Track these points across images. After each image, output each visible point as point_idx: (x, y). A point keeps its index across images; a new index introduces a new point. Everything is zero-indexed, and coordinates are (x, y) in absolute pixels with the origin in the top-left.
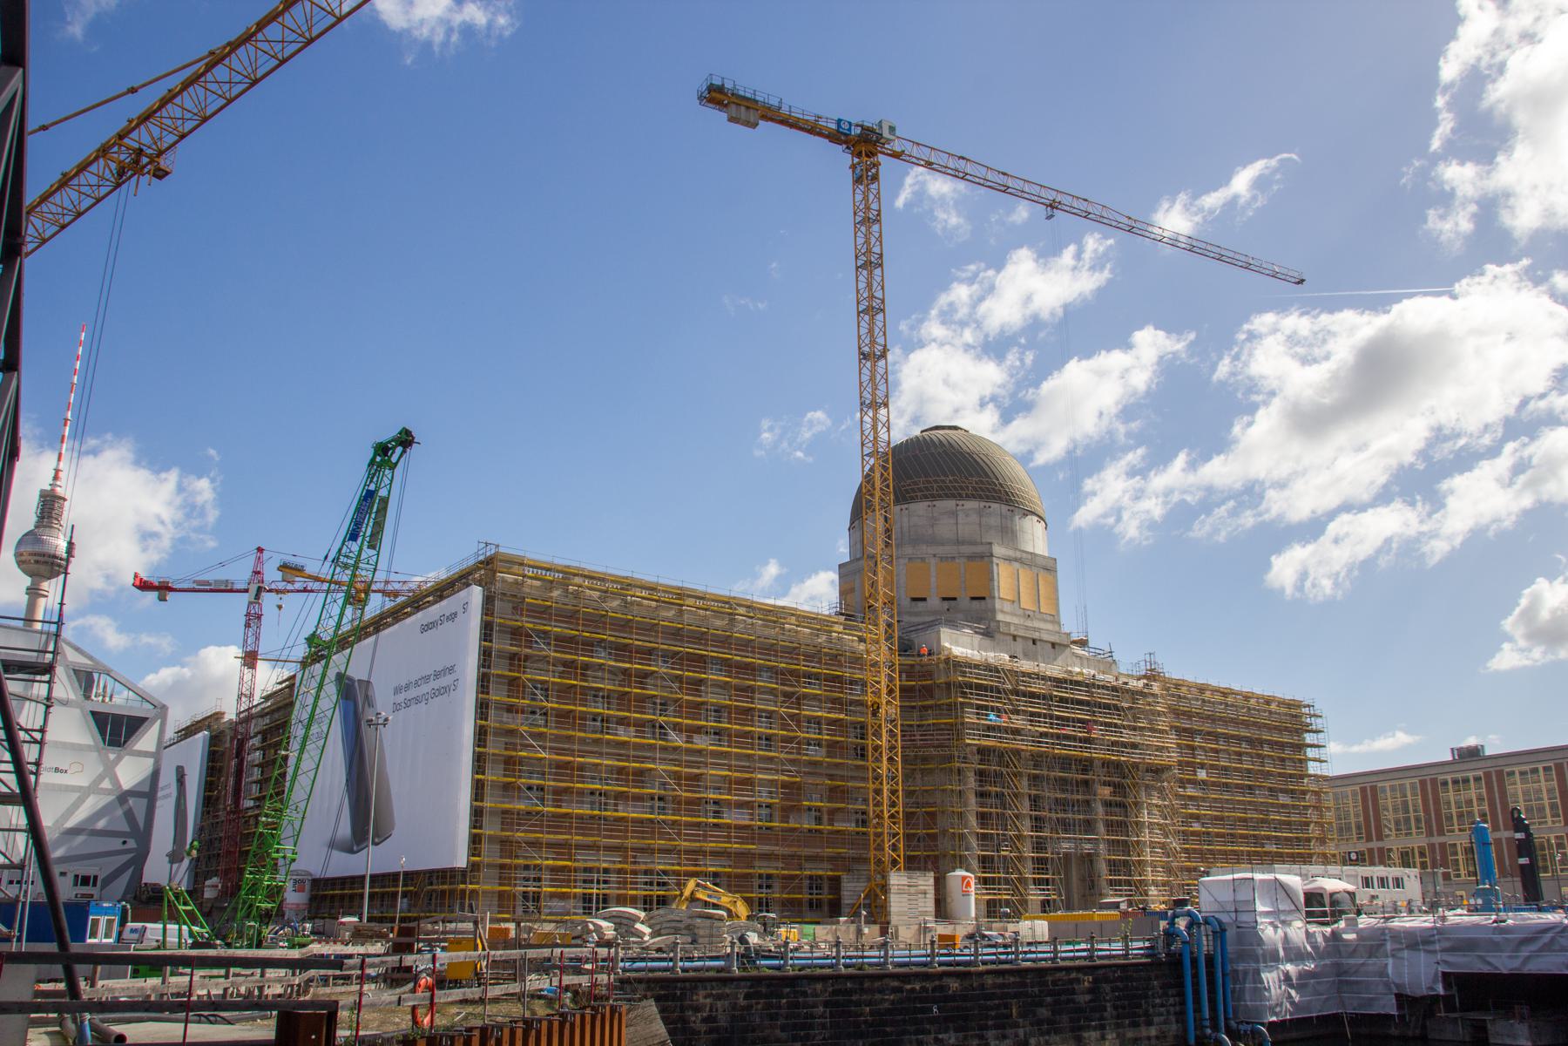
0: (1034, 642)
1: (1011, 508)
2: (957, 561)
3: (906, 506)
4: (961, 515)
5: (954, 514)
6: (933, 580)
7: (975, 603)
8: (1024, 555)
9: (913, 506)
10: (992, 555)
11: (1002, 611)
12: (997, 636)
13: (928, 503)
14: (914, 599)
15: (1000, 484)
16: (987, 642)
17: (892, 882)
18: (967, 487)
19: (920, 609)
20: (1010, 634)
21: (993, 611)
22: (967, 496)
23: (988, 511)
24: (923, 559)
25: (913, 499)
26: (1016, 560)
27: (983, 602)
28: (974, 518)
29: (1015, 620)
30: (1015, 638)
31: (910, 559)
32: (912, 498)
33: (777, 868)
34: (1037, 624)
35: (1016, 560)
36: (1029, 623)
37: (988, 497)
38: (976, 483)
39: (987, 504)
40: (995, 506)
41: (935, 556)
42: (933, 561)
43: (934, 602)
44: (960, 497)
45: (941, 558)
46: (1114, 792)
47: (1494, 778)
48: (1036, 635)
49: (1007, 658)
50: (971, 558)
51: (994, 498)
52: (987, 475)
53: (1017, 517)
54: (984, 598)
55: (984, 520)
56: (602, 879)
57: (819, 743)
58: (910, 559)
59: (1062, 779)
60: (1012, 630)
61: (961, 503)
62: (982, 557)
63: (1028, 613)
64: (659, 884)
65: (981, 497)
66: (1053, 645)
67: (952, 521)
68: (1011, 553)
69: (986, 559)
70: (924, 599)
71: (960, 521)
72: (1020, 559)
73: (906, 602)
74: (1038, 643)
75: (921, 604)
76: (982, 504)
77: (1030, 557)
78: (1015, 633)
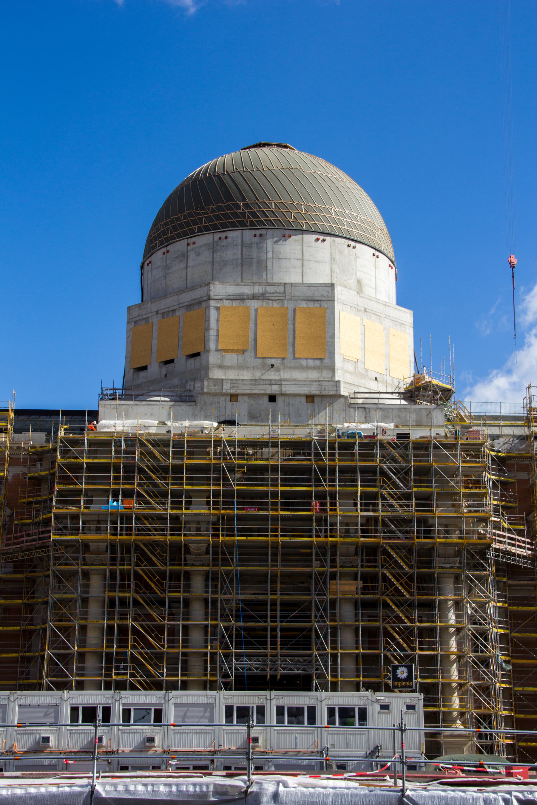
1: (258, 232)
2: (177, 313)
4: (192, 255)
5: (185, 256)
6: (155, 342)
7: (191, 361)
8: (270, 289)
10: (209, 299)
11: (221, 367)
12: (201, 399)
13: (164, 250)
15: (246, 205)
16: (184, 408)
20: (226, 394)
21: (206, 368)
22: (200, 230)
23: (224, 243)
24: (147, 319)
26: (254, 297)
27: (197, 359)
28: (206, 256)
29: (246, 375)
31: (136, 322)
34: (285, 375)
35: (254, 297)
36: (272, 375)
37: (224, 226)
39: (223, 235)
40: (234, 235)
41: (157, 312)
42: (155, 320)
43: (154, 369)
44: (192, 233)
45: (163, 313)
46: (364, 588)
47: (261, 512)
48: (274, 389)
49: (215, 424)
50: (190, 306)
51: (233, 225)
52: (229, 197)
53: (269, 242)
54: (198, 354)
55: (217, 256)
58: (136, 322)
59: (242, 574)
60: (227, 388)
61: (191, 241)
62: (200, 303)
63: (270, 362)
65: (215, 227)
66: (310, 398)
67: (183, 265)
68: (258, 289)
69: (204, 304)
70: (145, 368)
71: (191, 263)
72: (263, 294)
74: (279, 400)
76: (217, 236)
77: (281, 289)
78: (233, 391)
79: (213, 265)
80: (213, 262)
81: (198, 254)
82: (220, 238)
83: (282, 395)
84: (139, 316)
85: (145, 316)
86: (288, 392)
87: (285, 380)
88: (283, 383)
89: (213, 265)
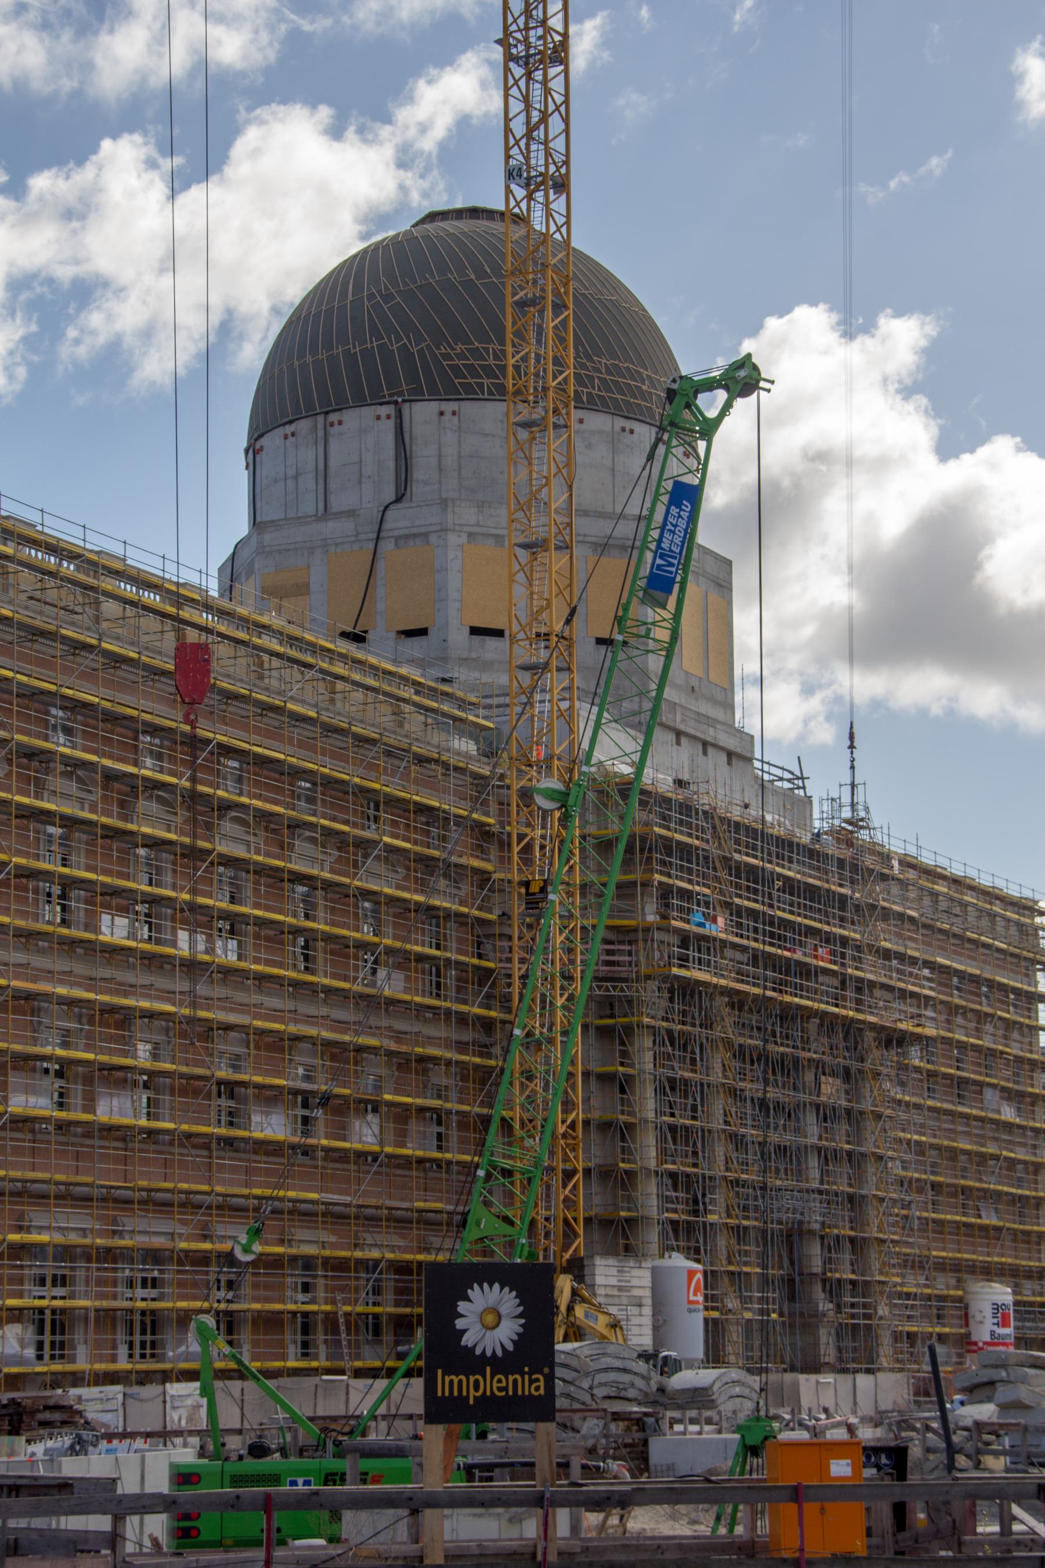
0: (705, 744)
3: (453, 406)
9: (469, 408)
14: (475, 631)
17: (599, 1280)
18: (591, 378)
19: (488, 656)
23: (627, 439)
25: (471, 393)
30: (679, 734)
31: (470, 535)
32: (468, 388)
33: (324, 1245)
38: (609, 372)
39: (629, 424)
56: (49, 1273)
57: (403, 960)
58: (470, 535)
64: (144, 1283)
66: (730, 755)
73: (459, 638)
75: (491, 642)
76: (620, 422)
78: (682, 727)
79: (614, 475)
80: (613, 470)
81: (589, 446)
82: (623, 429)
83: (715, 746)
84: (478, 525)
85: (495, 531)
86: (721, 744)
87: (719, 722)
88: (718, 726)
89: (614, 475)
